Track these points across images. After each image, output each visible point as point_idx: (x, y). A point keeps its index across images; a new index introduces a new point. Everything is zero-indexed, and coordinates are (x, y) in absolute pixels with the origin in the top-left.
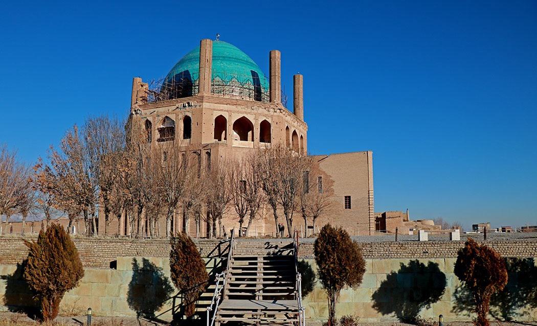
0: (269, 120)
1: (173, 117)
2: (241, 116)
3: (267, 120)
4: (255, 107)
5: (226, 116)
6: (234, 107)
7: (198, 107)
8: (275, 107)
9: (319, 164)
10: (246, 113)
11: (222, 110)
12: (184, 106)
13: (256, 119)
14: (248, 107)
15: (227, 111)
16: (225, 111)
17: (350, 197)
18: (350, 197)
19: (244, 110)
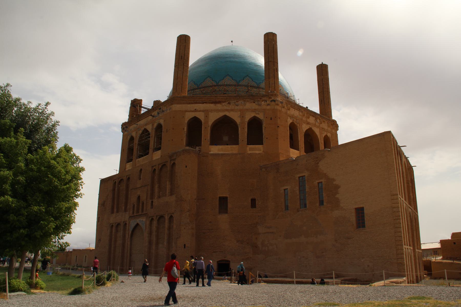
0: (261, 116)
1: (149, 128)
2: (221, 114)
3: (257, 116)
4: (240, 102)
5: (201, 116)
6: (212, 106)
7: (168, 111)
9: (318, 163)
10: (227, 110)
11: (196, 111)
12: (158, 113)
13: (242, 117)
14: (229, 103)
15: (203, 111)
16: (200, 111)
17: (362, 209)
18: (362, 209)
19: (225, 108)
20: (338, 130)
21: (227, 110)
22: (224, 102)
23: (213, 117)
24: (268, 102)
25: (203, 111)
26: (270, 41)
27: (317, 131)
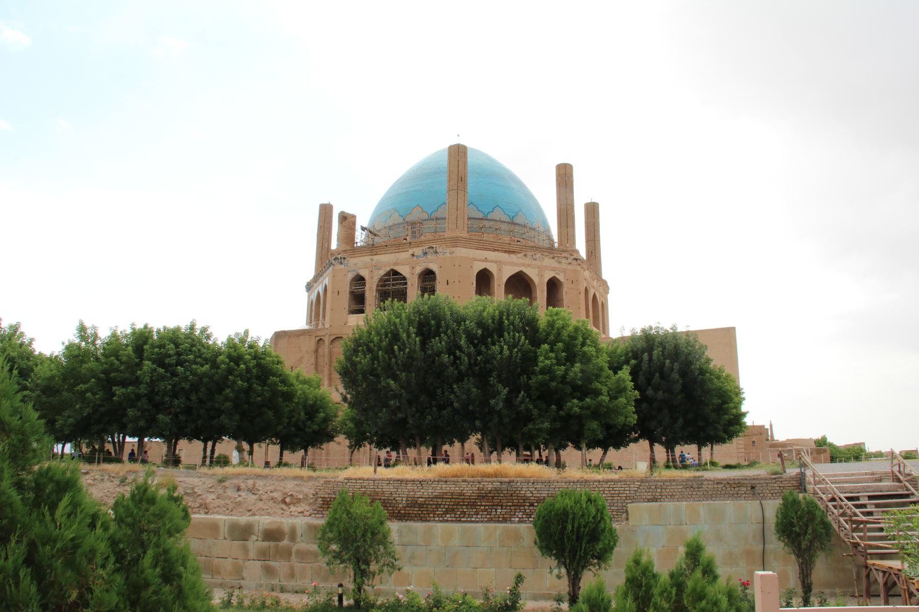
0: (561, 277)
1: (404, 271)
2: (516, 270)
3: (557, 276)
6: (506, 255)
7: (448, 255)
8: (568, 256)
10: (523, 265)
11: (486, 260)
14: (525, 255)
15: (496, 262)
19: (521, 261)
20: (607, 293)
21: (523, 265)
22: (519, 253)
23: (509, 272)
24: (570, 261)
25: (496, 262)
26: (564, 175)
27: (598, 295)
